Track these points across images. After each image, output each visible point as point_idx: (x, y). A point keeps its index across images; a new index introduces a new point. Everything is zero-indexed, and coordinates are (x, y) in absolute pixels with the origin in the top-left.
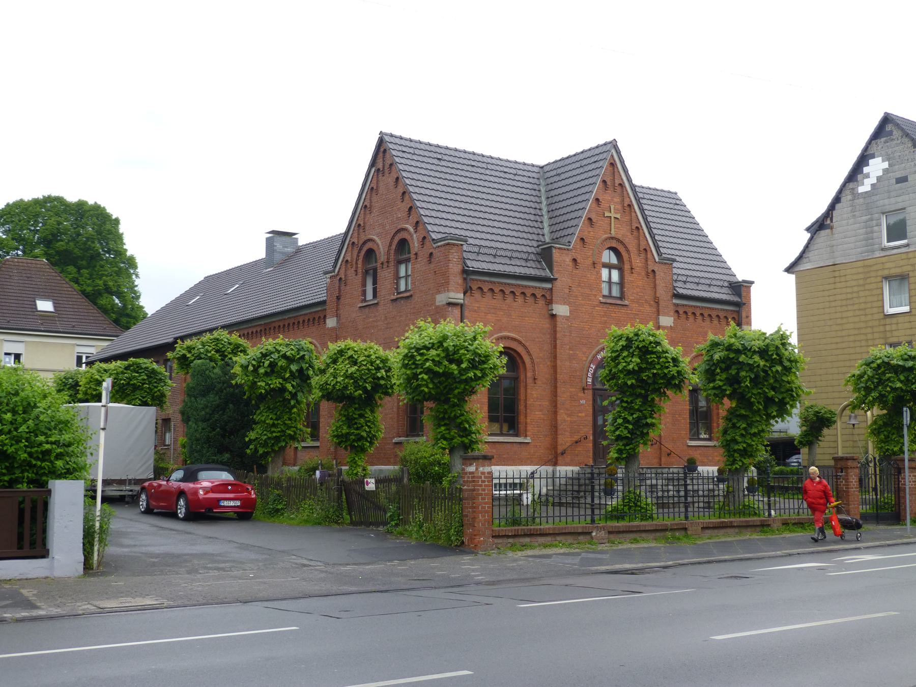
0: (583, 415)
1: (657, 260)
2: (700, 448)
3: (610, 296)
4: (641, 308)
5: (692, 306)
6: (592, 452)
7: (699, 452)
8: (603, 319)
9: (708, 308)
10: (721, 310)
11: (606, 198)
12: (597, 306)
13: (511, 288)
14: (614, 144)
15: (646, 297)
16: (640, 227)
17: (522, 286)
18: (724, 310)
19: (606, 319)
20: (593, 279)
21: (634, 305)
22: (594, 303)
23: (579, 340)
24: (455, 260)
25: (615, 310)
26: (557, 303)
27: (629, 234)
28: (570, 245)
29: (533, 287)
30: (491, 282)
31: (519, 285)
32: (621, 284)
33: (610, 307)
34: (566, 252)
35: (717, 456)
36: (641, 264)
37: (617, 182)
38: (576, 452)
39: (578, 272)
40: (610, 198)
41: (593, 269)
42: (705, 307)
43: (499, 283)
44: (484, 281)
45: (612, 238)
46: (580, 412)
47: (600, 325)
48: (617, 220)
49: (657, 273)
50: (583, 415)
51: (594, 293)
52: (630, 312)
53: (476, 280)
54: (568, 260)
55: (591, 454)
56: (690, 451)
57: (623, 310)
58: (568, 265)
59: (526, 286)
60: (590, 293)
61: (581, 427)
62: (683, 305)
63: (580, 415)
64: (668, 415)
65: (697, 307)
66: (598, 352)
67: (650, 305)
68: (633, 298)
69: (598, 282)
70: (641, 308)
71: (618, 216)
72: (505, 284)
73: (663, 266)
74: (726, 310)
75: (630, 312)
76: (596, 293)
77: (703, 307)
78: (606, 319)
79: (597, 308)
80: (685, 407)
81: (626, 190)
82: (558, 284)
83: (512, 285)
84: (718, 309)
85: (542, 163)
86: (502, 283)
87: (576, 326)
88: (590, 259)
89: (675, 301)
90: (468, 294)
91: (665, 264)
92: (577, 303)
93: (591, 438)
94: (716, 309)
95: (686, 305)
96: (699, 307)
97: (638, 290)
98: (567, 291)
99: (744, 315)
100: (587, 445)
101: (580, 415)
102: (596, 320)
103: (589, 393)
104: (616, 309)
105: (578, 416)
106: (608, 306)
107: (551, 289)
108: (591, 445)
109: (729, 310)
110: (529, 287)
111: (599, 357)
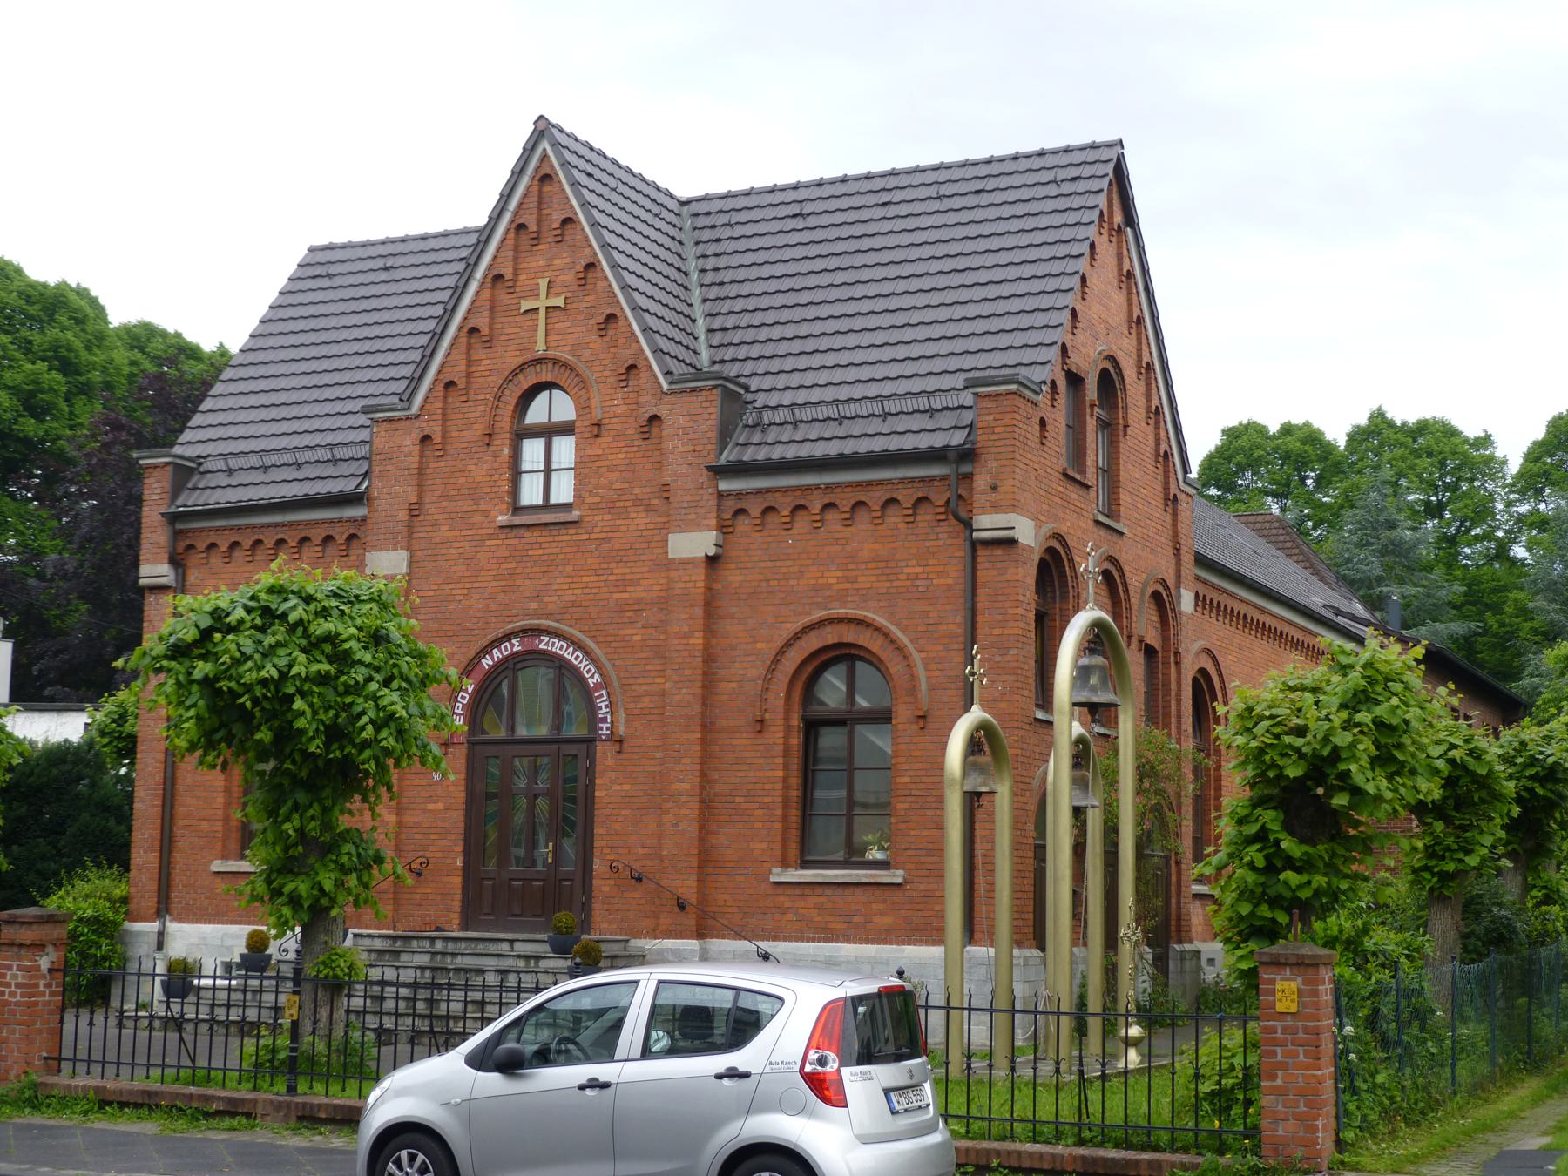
0: (440, 806)
1: (665, 387)
2: (819, 890)
3: (546, 506)
4: (618, 522)
5: (788, 490)
6: (459, 896)
7: (812, 900)
8: (505, 566)
9: (849, 484)
10: (902, 481)
11: (531, 265)
12: (490, 537)
13: (254, 533)
14: (543, 130)
15: (637, 491)
16: (618, 315)
17: (300, 523)
18: (912, 480)
19: (513, 565)
20: (483, 472)
21: (599, 518)
22: (481, 531)
23: (436, 626)
24: (154, 497)
25: (540, 539)
26: (376, 548)
27: (594, 337)
28: (409, 408)
29: (324, 522)
30: (232, 528)
31: (291, 524)
32: (516, 473)
33: (529, 534)
34: (408, 423)
35: (883, 914)
36: (625, 408)
37: (557, 217)
38: (418, 896)
39: (443, 464)
40: (541, 263)
41: (485, 448)
42: (839, 485)
43: (247, 527)
44: (217, 529)
45: (540, 361)
46: (430, 799)
47: (496, 584)
48: (557, 313)
49: (668, 421)
50: (440, 806)
51: (483, 507)
52: (586, 536)
53: (202, 530)
54: (408, 441)
55: (457, 904)
56: (782, 898)
57: (567, 536)
58: (409, 455)
59: (309, 523)
60: (475, 508)
61: (433, 837)
62: (759, 492)
63: (430, 806)
64: (684, 799)
65: (808, 488)
66: (486, 650)
67: (649, 509)
68: (597, 499)
69: (496, 477)
70: (618, 522)
71: (560, 302)
72: (262, 526)
73: (686, 398)
74: (922, 479)
75: (586, 536)
76: (490, 507)
77: (828, 487)
78: (513, 565)
79: (488, 543)
80: (772, 774)
81: (583, 229)
82: (382, 503)
83: (276, 525)
84: (890, 482)
85: (683, 193)
86: (254, 527)
87: (431, 593)
88: (475, 427)
89: (724, 486)
90: (193, 560)
91: (693, 390)
92: (438, 540)
93: (459, 863)
94: (880, 483)
95: (768, 490)
96: (817, 487)
97: (614, 476)
98: (403, 515)
99: (981, 482)
100: (446, 879)
101: (430, 806)
102: (483, 573)
103: (460, 753)
104: (544, 537)
105: (425, 811)
106: (522, 532)
107: (364, 519)
108: (459, 879)
109: (932, 479)
110: (316, 523)
111: (487, 662)
